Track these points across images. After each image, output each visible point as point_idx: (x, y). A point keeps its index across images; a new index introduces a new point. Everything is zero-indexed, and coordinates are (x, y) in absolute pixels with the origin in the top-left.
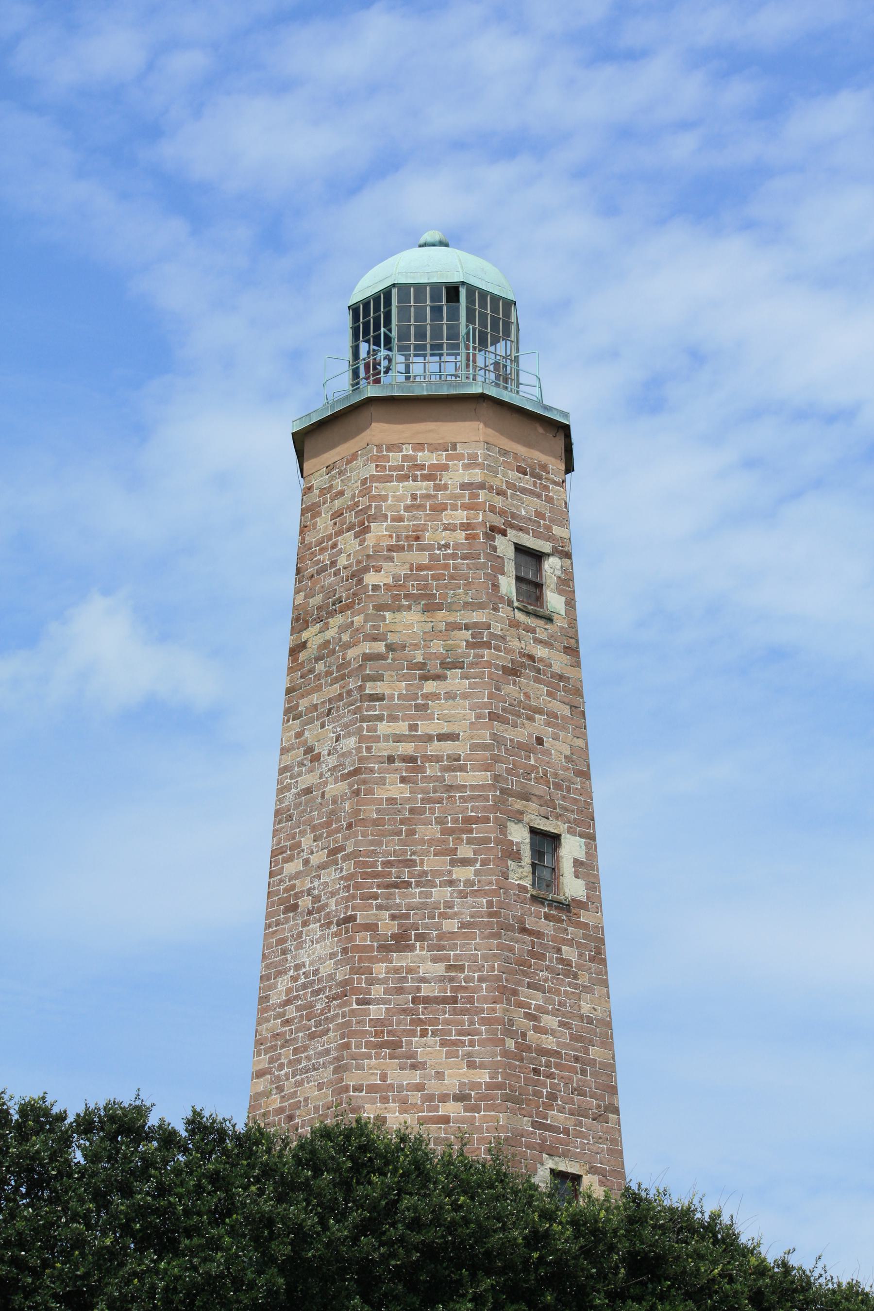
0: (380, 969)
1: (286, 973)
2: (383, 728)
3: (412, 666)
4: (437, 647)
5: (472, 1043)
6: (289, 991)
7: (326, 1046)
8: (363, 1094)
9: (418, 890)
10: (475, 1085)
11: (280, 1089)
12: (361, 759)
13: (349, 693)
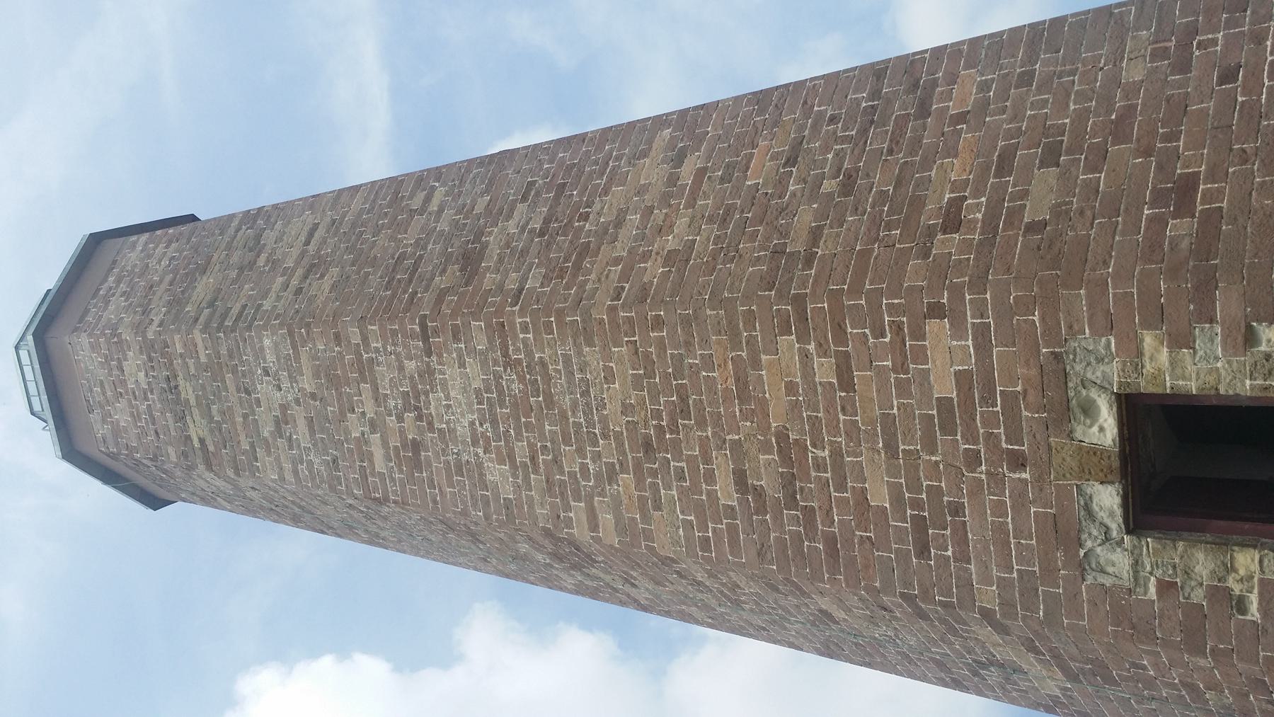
0: (489, 280)
1: (480, 465)
2: (267, 305)
3: (234, 281)
4: (235, 259)
5: (618, 158)
6: (502, 462)
7: (560, 367)
8: (627, 286)
9: (430, 246)
10: (671, 145)
11: (612, 476)
12: (281, 325)
13: (231, 356)
